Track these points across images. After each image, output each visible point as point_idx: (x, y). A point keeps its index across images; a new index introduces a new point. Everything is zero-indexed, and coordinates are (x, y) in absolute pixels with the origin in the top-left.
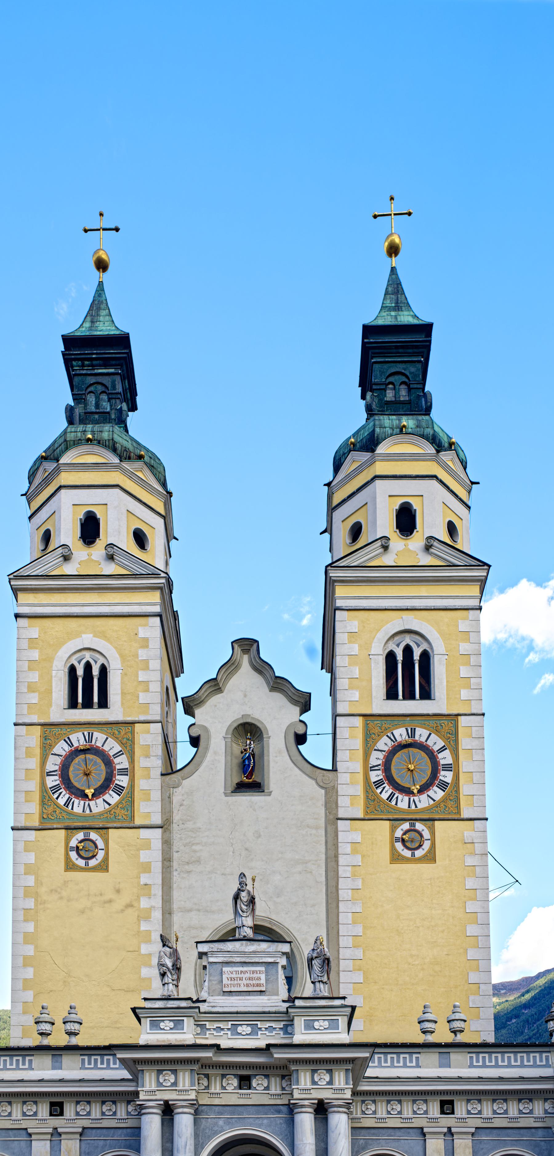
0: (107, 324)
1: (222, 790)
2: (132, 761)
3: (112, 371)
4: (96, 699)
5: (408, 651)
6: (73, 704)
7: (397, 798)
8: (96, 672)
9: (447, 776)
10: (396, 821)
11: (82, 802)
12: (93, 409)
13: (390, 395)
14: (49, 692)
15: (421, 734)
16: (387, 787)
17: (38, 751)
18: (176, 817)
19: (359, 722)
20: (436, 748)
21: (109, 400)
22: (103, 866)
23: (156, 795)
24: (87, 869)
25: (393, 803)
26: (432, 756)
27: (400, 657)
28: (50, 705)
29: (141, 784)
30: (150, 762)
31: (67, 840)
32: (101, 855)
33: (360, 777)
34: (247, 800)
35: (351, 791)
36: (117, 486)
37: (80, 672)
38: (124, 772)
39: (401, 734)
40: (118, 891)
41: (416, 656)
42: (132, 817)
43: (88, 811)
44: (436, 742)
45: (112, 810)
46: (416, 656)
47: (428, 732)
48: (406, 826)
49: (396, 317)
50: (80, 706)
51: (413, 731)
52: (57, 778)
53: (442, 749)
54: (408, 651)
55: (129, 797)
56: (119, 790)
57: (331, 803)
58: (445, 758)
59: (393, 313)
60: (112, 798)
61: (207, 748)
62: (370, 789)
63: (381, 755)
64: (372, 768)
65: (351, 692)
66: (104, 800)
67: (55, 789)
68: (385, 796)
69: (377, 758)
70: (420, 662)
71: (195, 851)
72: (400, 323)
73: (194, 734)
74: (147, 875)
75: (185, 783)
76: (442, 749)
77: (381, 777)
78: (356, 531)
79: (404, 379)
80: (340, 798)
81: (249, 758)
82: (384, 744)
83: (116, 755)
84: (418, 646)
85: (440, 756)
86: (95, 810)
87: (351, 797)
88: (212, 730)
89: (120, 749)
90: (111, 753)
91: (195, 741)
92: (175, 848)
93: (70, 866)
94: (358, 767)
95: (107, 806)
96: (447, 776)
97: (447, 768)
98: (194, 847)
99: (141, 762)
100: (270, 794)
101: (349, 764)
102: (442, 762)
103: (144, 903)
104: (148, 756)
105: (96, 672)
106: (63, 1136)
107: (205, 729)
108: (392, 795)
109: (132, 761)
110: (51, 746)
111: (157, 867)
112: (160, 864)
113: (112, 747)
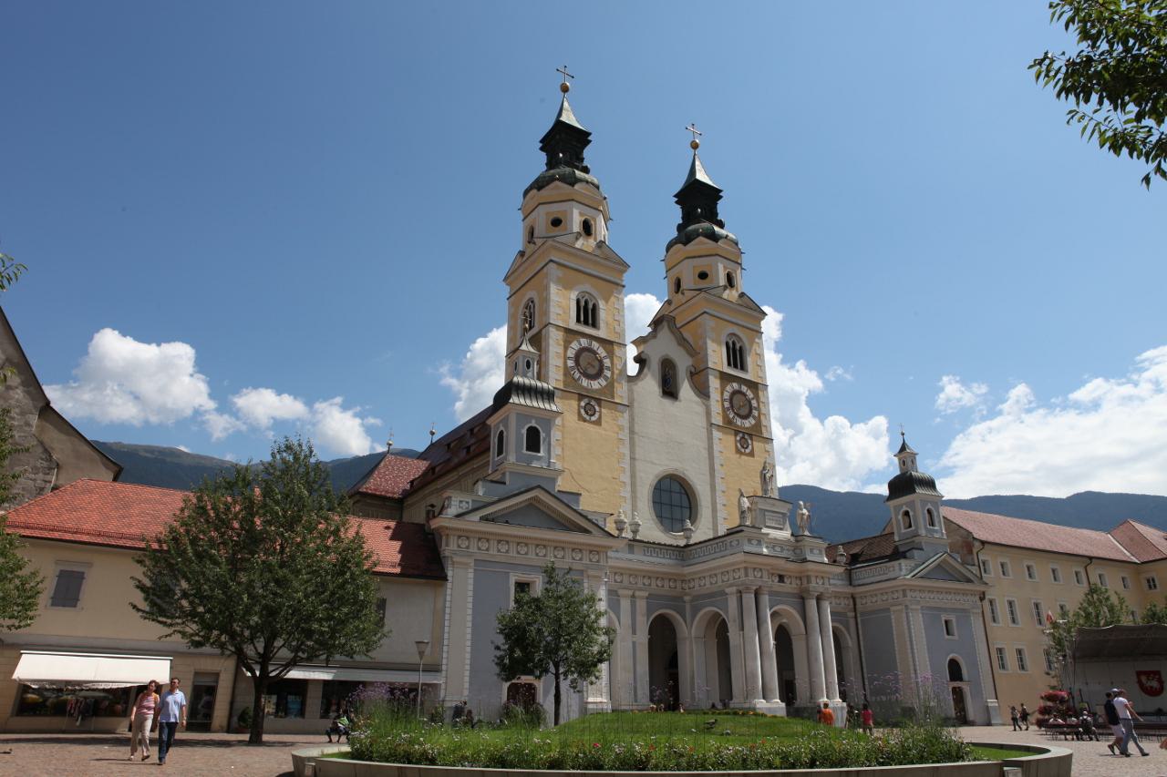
15: (744, 389)
24: (590, 422)
34: (667, 402)
36: (573, 200)
38: (608, 368)
42: (613, 397)
53: (753, 399)
55: (610, 388)
57: (708, 414)
62: (724, 410)
63: (728, 394)
68: (731, 416)
73: (643, 356)
76: (753, 399)
89: (606, 354)
91: (638, 359)
96: (755, 413)
100: (680, 401)
109: (612, 363)
110: (570, 343)
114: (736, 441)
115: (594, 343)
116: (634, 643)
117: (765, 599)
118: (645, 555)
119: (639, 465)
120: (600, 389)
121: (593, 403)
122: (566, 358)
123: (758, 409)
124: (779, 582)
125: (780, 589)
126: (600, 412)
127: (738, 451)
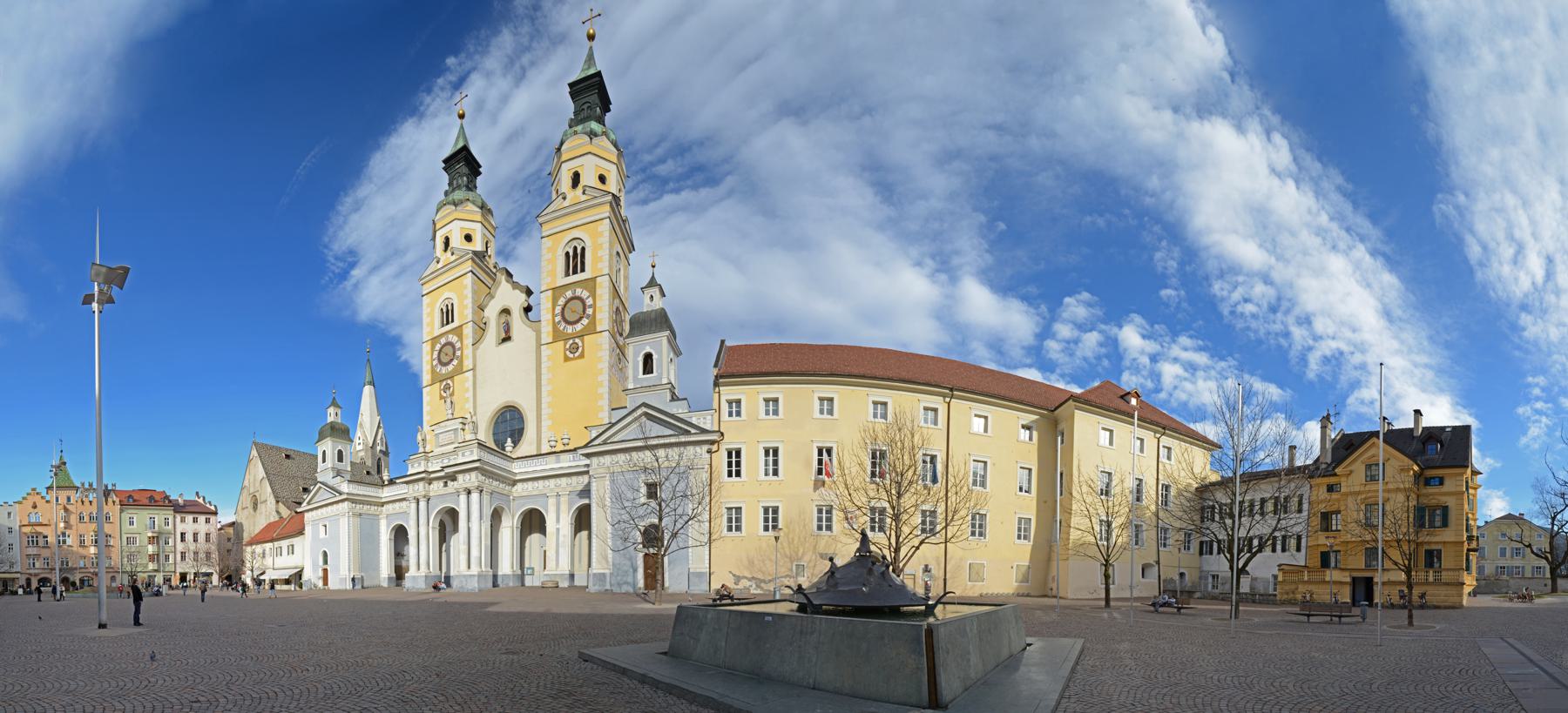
10: (566, 340)
15: (579, 292)
30: (468, 341)
39: (569, 294)
44: (585, 294)
58: (589, 302)
60: (455, 362)
62: (555, 325)
69: (558, 310)
87: (547, 336)
96: (589, 311)
113: (453, 338)
117: (423, 504)
123: (593, 306)
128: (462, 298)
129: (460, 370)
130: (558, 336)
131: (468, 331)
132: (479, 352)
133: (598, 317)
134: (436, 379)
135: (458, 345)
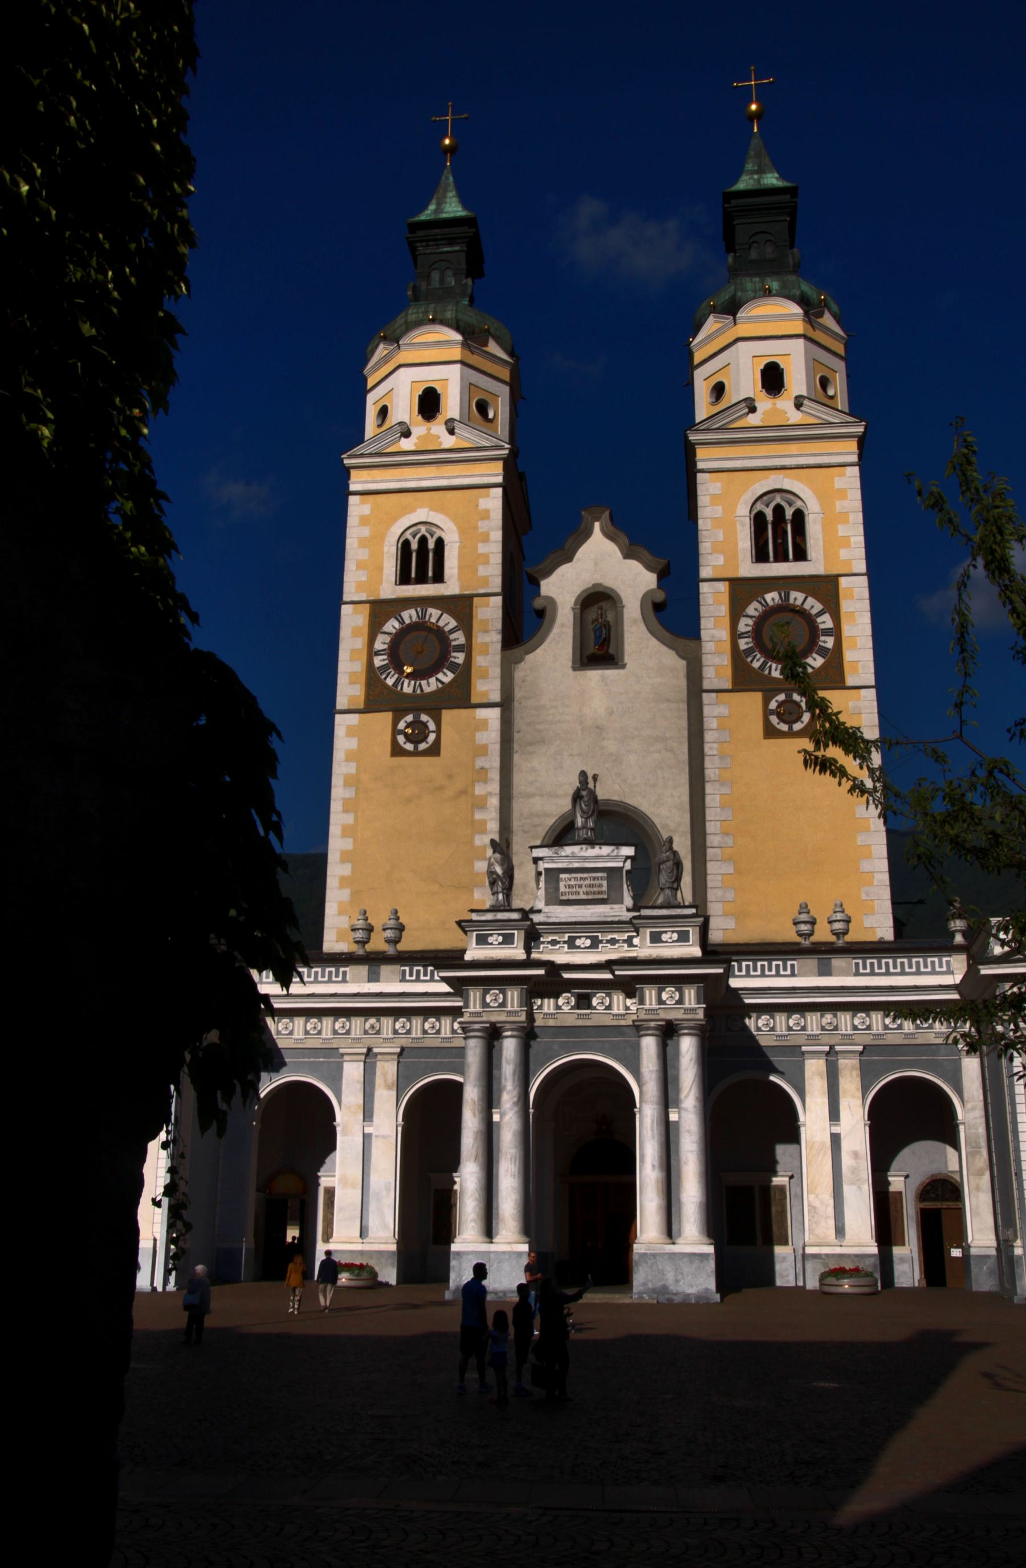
0: (453, 205)
1: (570, 664)
2: (469, 636)
3: (457, 248)
4: (430, 574)
5: (779, 510)
6: (404, 578)
7: (770, 667)
8: (431, 545)
9: (829, 642)
11: (413, 682)
12: (437, 285)
13: (753, 255)
14: (380, 569)
15: (797, 597)
16: (759, 656)
17: (365, 630)
18: (518, 694)
19: (723, 587)
20: (814, 612)
21: (455, 275)
22: (435, 750)
23: (496, 671)
25: (766, 672)
26: (809, 620)
27: (770, 517)
28: (380, 582)
29: (480, 661)
31: (395, 723)
32: (432, 737)
33: (727, 646)
35: (717, 660)
37: (414, 546)
38: (459, 648)
39: (772, 597)
40: (450, 777)
41: (789, 513)
43: (419, 692)
44: (813, 606)
45: (445, 689)
46: (789, 513)
47: (804, 595)
48: (782, 697)
49: (759, 180)
50: (413, 581)
51: (787, 596)
52: (385, 657)
53: (820, 614)
54: (779, 510)
55: (464, 674)
56: (453, 667)
58: (826, 621)
59: (756, 177)
61: (553, 621)
62: (738, 658)
63: (750, 622)
64: (742, 636)
65: (714, 556)
66: (438, 680)
67: (383, 668)
68: (756, 665)
69: (745, 625)
70: (793, 522)
71: (539, 731)
72: (763, 187)
74: (483, 758)
75: (529, 657)
77: (751, 645)
78: (719, 390)
79: (769, 237)
80: (705, 670)
81: (600, 629)
82: (753, 609)
83: (452, 631)
84: (790, 505)
85: (819, 620)
86: (427, 690)
88: (559, 600)
90: (447, 629)
92: (516, 728)
93: (397, 751)
94: (724, 634)
95: (440, 685)
97: (827, 632)
98: (537, 727)
99: (479, 638)
100: (624, 667)
101: (713, 631)
102: (821, 626)
103: (479, 790)
104: (486, 631)
105: (431, 545)
106: (379, 1057)
107: (551, 601)
108: (764, 664)
111: (495, 749)
112: (498, 747)
113: (448, 622)
114: (767, 713)
115: (430, 610)
116: (367, 1138)
117: (509, 1047)
118: (403, 980)
119: (518, 807)
120: (438, 691)
121: (424, 718)
122: (372, 653)
123: (836, 632)
124: (578, 1006)
125: (580, 1023)
126: (438, 732)
127: (770, 732)
128: (469, 533)
129: (458, 695)
130: (744, 679)
131: (490, 613)
132: (521, 672)
133: (848, 656)
134: (377, 698)
135: (458, 638)
